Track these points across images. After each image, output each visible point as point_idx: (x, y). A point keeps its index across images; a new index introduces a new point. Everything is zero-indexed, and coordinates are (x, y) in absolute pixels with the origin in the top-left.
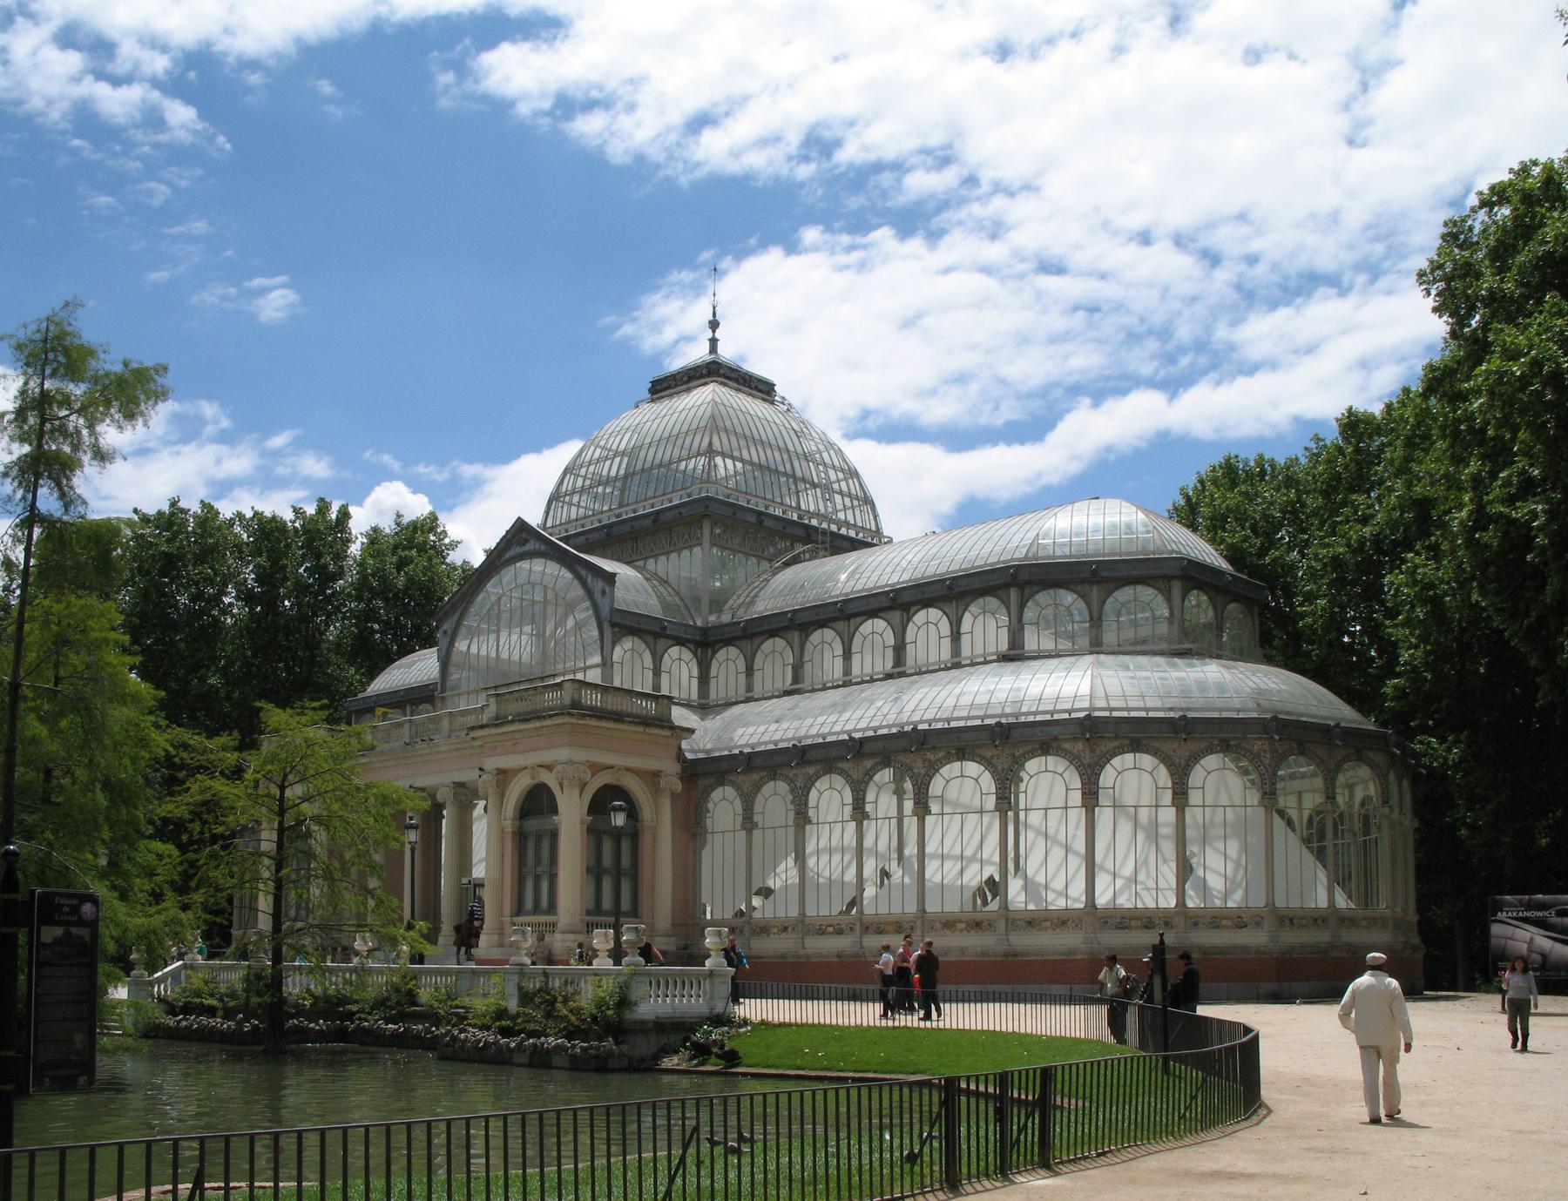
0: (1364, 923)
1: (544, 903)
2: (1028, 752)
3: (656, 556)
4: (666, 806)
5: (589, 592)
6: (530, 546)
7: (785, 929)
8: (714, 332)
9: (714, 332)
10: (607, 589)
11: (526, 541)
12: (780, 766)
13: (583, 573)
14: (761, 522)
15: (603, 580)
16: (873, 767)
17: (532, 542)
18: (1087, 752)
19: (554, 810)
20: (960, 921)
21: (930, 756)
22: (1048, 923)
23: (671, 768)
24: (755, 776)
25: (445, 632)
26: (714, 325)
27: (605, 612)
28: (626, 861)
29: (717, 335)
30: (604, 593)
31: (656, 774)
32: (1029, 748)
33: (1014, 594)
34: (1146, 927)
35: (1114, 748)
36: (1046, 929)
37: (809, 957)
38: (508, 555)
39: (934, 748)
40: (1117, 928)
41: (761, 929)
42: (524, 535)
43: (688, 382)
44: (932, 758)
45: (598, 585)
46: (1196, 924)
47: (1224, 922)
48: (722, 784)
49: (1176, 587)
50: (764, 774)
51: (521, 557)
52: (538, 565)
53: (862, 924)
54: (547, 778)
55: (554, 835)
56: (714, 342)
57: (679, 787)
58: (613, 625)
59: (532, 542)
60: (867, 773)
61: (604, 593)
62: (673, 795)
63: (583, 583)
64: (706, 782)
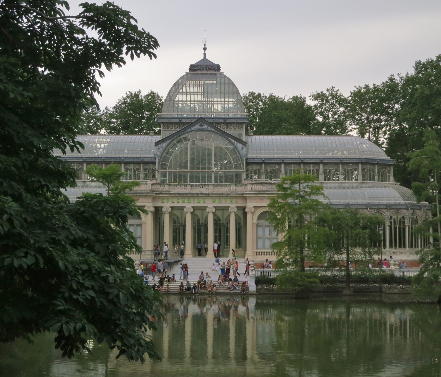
8: (205, 51)
9: (205, 51)
11: (201, 125)
13: (233, 141)
15: (242, 144)
22: (398, 253)
26: (205, 49)
29: (206, 52)
38: (193, 128)
43: (207, 70)
45: (240, 146)
51: (201, 130)
56: (205, 54)
61: (242, 148)
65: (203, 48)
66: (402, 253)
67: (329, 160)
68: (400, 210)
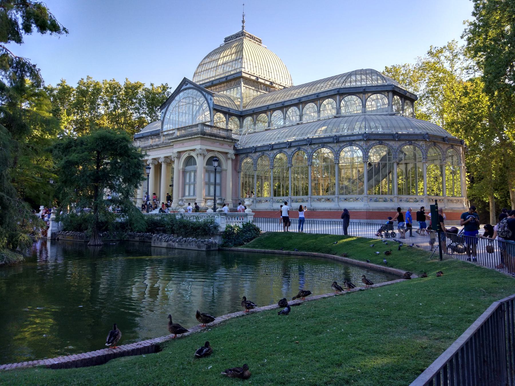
0: (455, 201)
1: (192, 194)
2: (345, 145)
3: (226, 90)
4: (230, 162)
5: (207, 100)
6: (188, 86)
7: (267, 201)
10: (212, 98)
11: (187, 84)
12: (265, 150)
13: (205, 93)
14: (258, 79)
16: (294, 151)
17: (189, 84)
18: (365, 144)
19: (195, 164)
20: (323, 199)
21: (313, 146)
22: (352, 200)
23: (231, 151)
24: (258, 154)
25: (163, 113)
26: (243, 22)
27: (212, 106)
28: (218, 181)
30: (211, 99)
31: (227, 153)
32: (345, 144)
33: (338, 97)
34: (385, 201)
35: (373, 144)
36: (351, 201)
37: (274, 210)
39: (314, 144)
40: (375, 201)
41: (259, 201)
42: (186, 82)
44: (314, 147)
45: (209, 97)
46: (401, 201)
47: (411, 200)
48: (247, 157)
49: (390, 94)
50: (260, 153)
51: (185, 89)
52: (190, 90)
53: (291, 200)
54: (193, 154)
55: (195, 171)
56: (243, 27)
57: (234, 157)
58: (215, 109)
59: (189, 84)
60: (293, 152)
62: (232, 160)
63: (205, 96)
64: (242, 156)
65: (242, 21)
66: (357, 199)
67: (306, 98)
68: (354, 143)
